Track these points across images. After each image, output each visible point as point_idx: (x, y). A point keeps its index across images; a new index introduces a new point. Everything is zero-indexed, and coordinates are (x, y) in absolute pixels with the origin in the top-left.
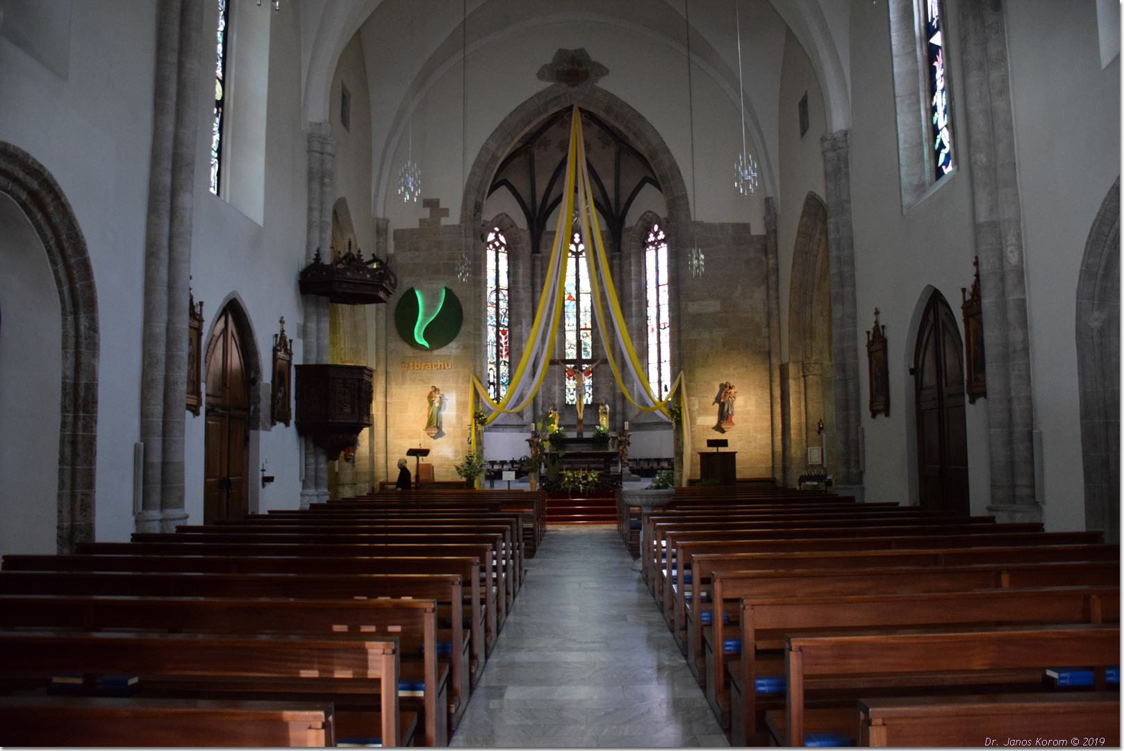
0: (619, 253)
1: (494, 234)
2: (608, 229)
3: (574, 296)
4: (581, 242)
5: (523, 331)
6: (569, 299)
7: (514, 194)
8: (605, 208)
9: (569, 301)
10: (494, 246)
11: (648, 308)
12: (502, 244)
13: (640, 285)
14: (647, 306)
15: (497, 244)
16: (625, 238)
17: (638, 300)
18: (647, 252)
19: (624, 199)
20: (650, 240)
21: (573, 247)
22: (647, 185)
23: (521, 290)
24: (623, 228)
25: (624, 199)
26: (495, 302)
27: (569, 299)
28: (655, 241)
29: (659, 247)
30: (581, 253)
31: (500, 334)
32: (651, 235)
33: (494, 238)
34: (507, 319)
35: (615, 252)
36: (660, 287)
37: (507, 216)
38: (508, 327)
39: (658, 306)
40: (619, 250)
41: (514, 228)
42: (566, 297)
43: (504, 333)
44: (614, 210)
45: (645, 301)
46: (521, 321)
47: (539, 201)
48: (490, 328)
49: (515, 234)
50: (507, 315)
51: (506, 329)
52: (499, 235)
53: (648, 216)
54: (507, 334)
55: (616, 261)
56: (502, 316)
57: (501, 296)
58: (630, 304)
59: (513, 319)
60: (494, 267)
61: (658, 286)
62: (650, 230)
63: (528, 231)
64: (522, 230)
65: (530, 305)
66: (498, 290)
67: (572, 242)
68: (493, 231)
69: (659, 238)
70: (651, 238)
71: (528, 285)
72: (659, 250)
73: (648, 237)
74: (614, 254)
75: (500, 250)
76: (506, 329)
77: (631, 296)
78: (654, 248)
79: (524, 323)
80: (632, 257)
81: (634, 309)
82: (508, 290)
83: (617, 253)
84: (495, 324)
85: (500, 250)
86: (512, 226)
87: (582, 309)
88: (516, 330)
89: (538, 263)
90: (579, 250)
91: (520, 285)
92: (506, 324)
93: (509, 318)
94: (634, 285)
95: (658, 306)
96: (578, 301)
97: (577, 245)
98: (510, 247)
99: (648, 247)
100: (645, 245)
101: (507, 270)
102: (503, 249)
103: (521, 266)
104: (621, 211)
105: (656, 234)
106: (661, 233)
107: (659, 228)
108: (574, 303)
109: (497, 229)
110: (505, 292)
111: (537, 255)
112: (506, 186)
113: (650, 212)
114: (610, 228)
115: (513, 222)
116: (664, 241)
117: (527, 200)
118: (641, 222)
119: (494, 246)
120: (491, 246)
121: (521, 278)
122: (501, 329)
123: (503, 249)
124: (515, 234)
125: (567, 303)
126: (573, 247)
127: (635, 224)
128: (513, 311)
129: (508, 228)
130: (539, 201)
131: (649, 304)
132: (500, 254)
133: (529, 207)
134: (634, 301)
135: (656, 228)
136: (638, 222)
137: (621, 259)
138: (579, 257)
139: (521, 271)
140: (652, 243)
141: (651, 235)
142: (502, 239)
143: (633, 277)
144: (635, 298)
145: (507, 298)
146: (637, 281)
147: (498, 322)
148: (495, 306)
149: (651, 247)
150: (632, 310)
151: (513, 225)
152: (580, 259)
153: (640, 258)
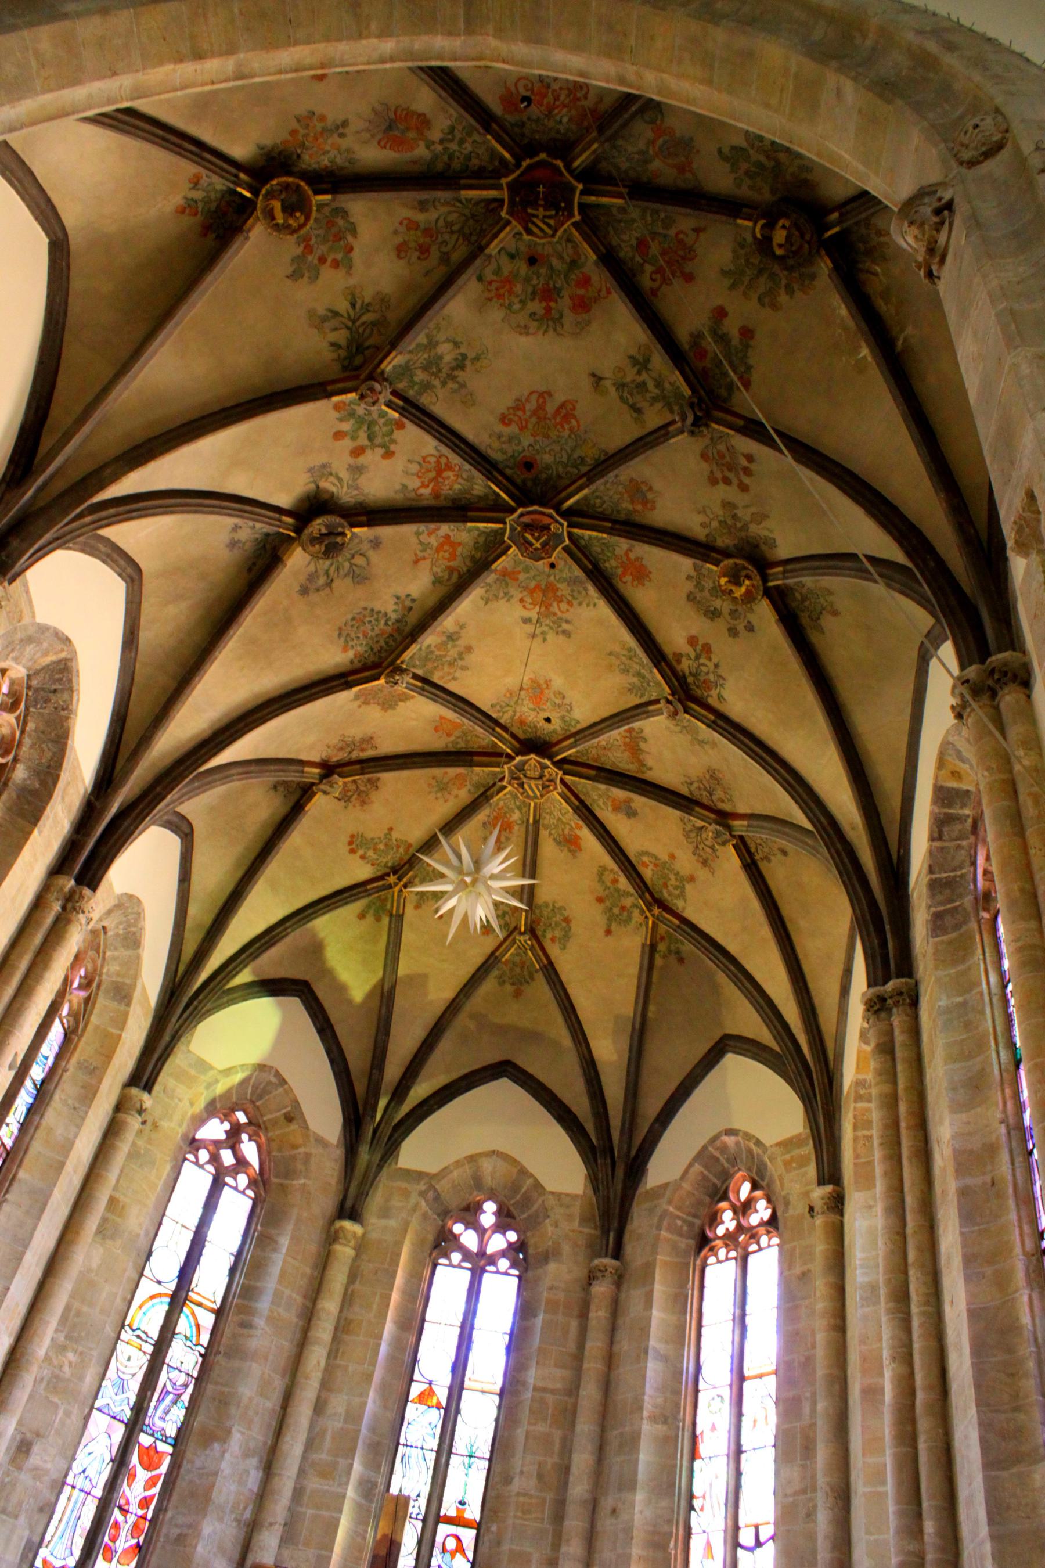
0: (615, 1263)
1: (227, 1126)
2: (590, 1192)
3: (442, 1394)
4: (501, 1227)
5: (225, 1467)
6: (422, 1398)
7: (321, 1032)
8: (590, 1127)
9: (422, 1408)
10: (215, 1159)
11: (697, 1464)
12: (241, 1163)
13: (677, 1374)
14: (694, 1455)
15: (227, 1158)
16: (640, 1220)
17: (660, 1429)
18: (708, 1270)
19: (651, 1106)
20: (720, 1231)
21: (469, 1239)
22: (731, 1060)
23: (260, 1322)
24: (641, 1190)
25: (651, 1106)
26: (155, 1334)
27: (422, 1398)
28: (740, 1228)
29: (753, 1247)
30: (492, 1260)
31: (135, 1459)
32: (728, 1216)
33: (223, 1136)
34: (178, 1414)
35: (600, 1256)
36: (747, 1385)
37: (283, 1082)
38: (179, 1441)
39: (737, 1452)
40: (617, 1253)
41: (294, 1126)
42: (416, 1390)
43: (150, 1458)
44: (616, 1135)
45: (687, 1435)
46: (229, 1432)
47: (393, 1071)
48: (98, 1422)
49: (295, 1147)
50: (186, 1398)
51: (162, 1447)
52: (244, 1137)
53: (724, 1148)
54: (163, 1469)
55: (601, 1289)
56: (165, 1393)
57: (184, 1325)
58: (632, 1442)
59: (200, 1420)
60: (193, 1223)
61: (740, 1378)
62: (725, 1197)
63: (339, 1153)
64: (320, 1141)
65: (279, 1384)
66: (179, 1299)
67: (473, 1224)
68: (226, 1115)
69: (754, 1220)
70: (728, 1222)
71: (291, 1316)
72: (752, 1260)
73: (714, 1219)
74: (596, 1262)
75: (228, 1180)
76: (162, 1447)
77: (641, 1408)
78: (733, 1254)
79: (237, 1439)
80: (657, 1277)
81: (646, 1457)
82: (219, 1313)
83: (607, 1261)
84: (128, 1414)
85: (228, 1180)
86: (289, 1119)
87: (460, 1445)
88: (196, 1459)
89: (344, 1252)
90: (489, 1251)
91: (264, 1304)
92: (172, 1432)
93: (191, 1410)
94: (653, 1369)
95: (737, 1452)
96: (451, 1412)
97: (481, 1231)
98: (265, 1183)
99: (713, 1250)
100: (703, 1242)
101: (235, 1249)
102: (243, 1180)
103: (284, 1242)
104: (637, 1142)
105: (745, 1208)
106: (762, 1204)
107: (755, 1186)
108: (436, 1417)
109: (241, 1117)
110: (207, 1320)
111: (348, 1225)
112: (302, 1001)
113: (730, 1132)
114: (596, 1190)
115: (296, 1102)
116: (773, 1222)
117: (357, 1055)
118: (697, 1167)
119: (215, 1159)
120: (204, 1155)
121: (271, 1283)
122: (145, 1440)
123: (243, 1180)
124: (295, 1147)
125: (412, 1411)
126: (469, 1239)
127: (677, 1175)
128: (210, 1389)
129: (275, 1122)
130: (393, 1071)
131: (703, 1449)
132: (227, 1193)
133: (360, 1088)
134: (646, 1428)
135: (745, 1189)
136: (690, 1165)
137: (619, 1280)
138: (483, 1271)
139: (278, 1261)
140: (730, 1239)
141: (728, 1216)
142: (249, 1150)
143: (653, 1343)
144: (653, 1419)
145: (205, 1339)
146: (665, 1359)
147: (140, 1409)
148: (150, 1349)
149: (722, 1253)
150: (637, 1460)
151: (293, 1116)
152: (486, 1276)
153: (683, 1284)
